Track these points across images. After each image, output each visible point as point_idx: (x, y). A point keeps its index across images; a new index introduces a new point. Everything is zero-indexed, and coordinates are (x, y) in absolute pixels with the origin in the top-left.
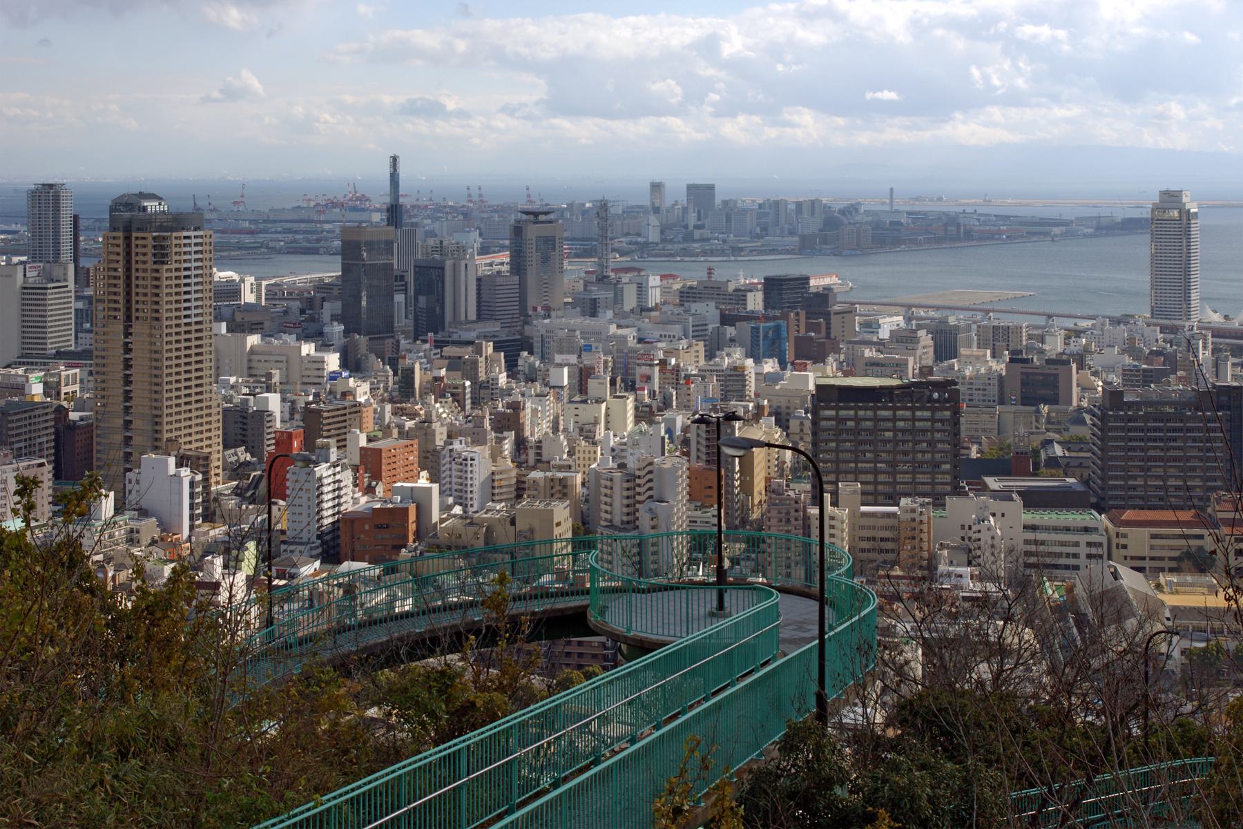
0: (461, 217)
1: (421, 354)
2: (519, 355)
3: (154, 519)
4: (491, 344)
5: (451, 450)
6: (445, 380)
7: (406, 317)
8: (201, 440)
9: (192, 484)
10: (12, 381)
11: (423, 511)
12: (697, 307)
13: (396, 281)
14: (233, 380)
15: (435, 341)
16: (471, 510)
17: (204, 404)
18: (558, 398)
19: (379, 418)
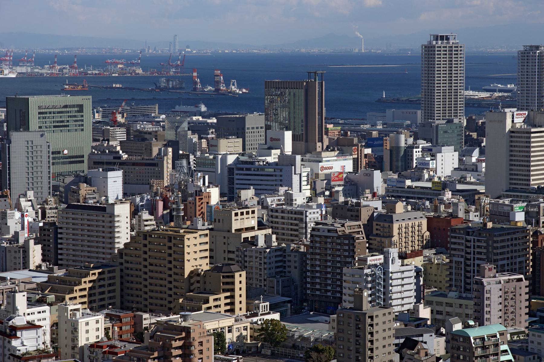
10: (500, 209)
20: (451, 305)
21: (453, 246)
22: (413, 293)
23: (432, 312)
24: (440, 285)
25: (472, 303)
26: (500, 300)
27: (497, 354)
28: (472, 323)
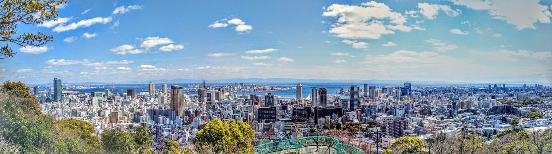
12: (242, 98)
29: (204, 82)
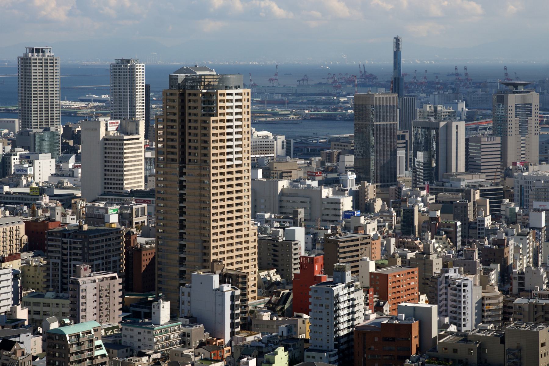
0: (450, 91)
1: (419, 199)
2: (501, 202)
3: (202, 326)
4: (478, 191)
5: (447, 278)
6: (440, 220)
7: (407, 169)
8: (241, 262)
9: (233, 298)
10: (95, 212)
11: (425, 327)
13: (399, 139)
14: (267, 216)
15: (431, 189)
16: (463, 330)
17: (243, 233)
18: (537, 238)
19: (386, 250)
20: (47, 305)
21: (50, 249)
22: (11, 296)
23: (29, 312)
24: (38, 286)
25: (68, 302)
26: (95, 298)
27: (91, 350)
28: (67, 321)
29: (397, 55)
